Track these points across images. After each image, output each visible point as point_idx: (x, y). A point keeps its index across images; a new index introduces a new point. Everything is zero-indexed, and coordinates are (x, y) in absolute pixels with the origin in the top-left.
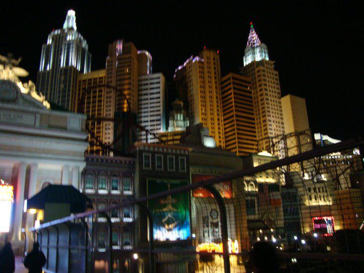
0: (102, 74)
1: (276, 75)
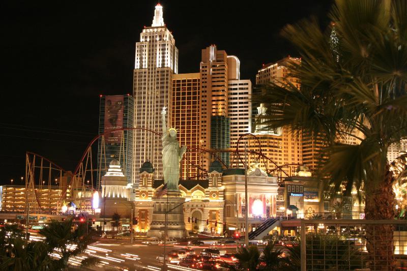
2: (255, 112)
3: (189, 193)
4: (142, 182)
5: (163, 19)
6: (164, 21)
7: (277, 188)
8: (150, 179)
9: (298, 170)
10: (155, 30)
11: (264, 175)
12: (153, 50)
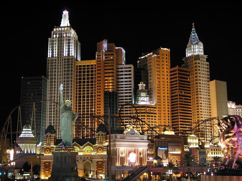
0: (93, 62)
1: (207, 65)
2: (136, 87)
3: (82, 148)
4: (47, 140)
5: (68, 21)
6: (70, 22)
7: (147, 144)
8: (52, 139)
9: (165, 130)
10: (63, 29)
11: (137, 134)
12: (61, 44)
